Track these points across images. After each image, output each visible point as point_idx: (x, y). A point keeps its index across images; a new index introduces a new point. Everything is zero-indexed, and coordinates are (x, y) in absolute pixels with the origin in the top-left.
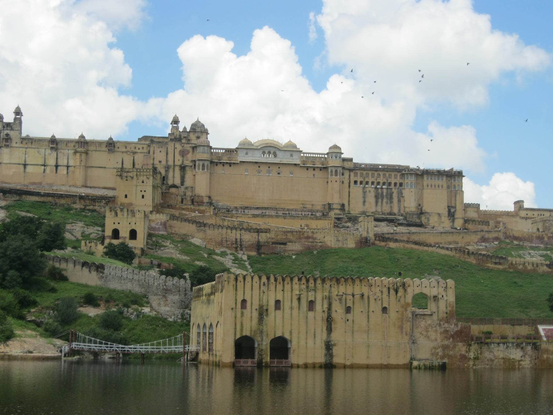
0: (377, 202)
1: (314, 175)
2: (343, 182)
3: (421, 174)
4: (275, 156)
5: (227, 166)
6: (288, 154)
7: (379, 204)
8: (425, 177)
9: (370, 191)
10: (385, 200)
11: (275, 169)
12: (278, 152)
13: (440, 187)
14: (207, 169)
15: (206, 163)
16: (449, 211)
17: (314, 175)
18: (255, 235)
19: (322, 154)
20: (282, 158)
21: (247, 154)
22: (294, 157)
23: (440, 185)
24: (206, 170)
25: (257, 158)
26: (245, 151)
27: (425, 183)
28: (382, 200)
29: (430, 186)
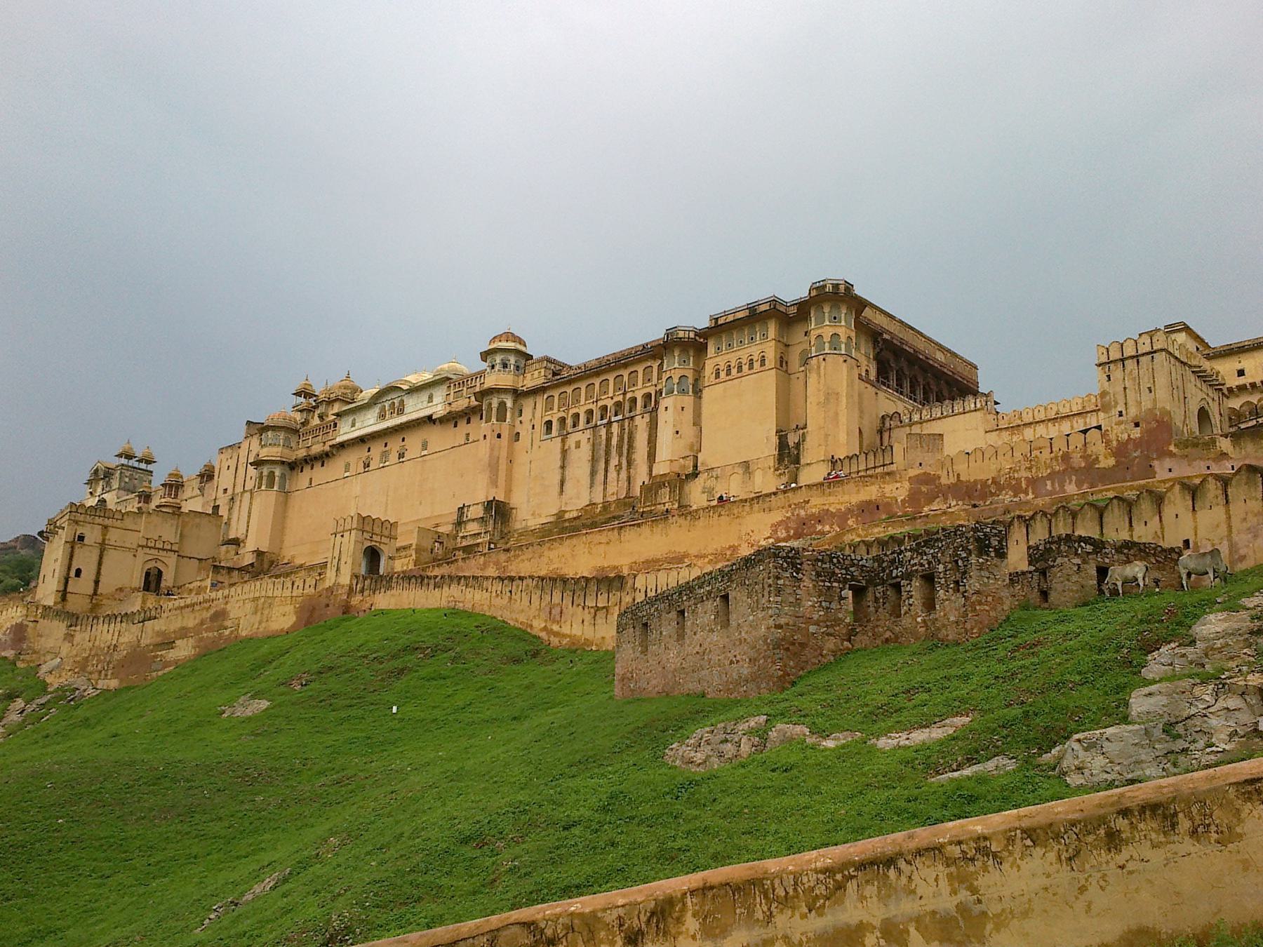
0: (593, 473)
4: (401, 411)
5: (318, 465)
7: (600, 477)
8: (711, 350)
9: (578, 445)
10: (614, 461)
11: (395, 445)
13: (757, 365)
14: (271, 484)
15: (266, 471)
16: (783, 445)
17: (468, 435)
18: (135, 629)
20: (416, 408)
21: (353, 425)
22: (436, 400)
24: (263, 487)
28: (607, 462)
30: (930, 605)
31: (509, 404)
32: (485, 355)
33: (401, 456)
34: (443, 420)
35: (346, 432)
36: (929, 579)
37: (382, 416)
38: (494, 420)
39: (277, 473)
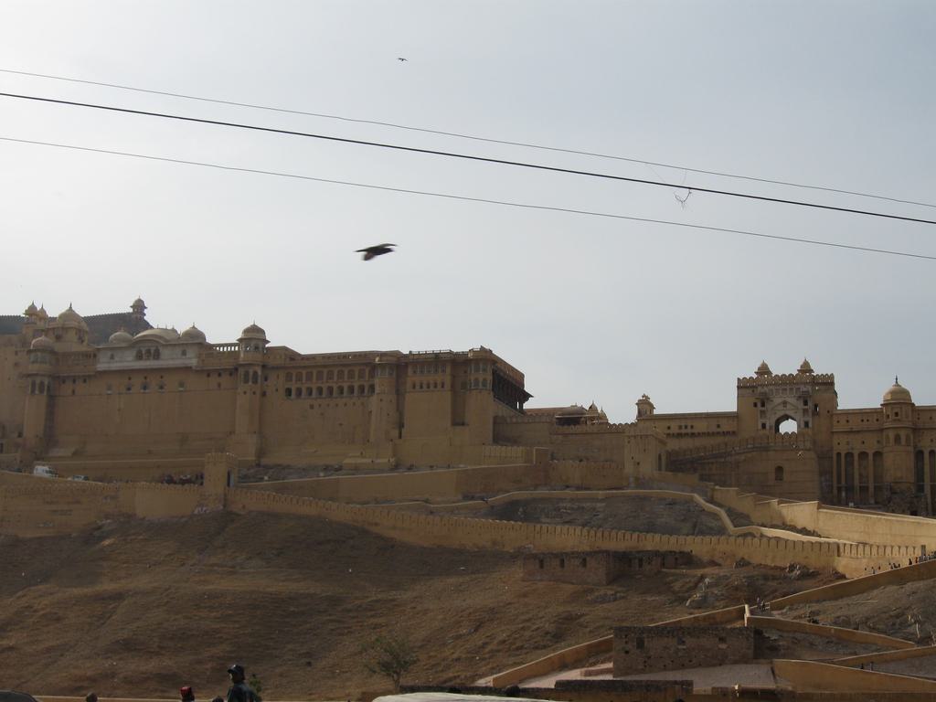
1: (219, 385)
2: (264, 394)
3: (399, 366)
4: (157, 356)
6: (178, 351)
8: (410, 371)
9: (312, 407)
12: (161, 349)
13: (439, 386)
17: (219, 385)
19: (231, 345)
20: (169, 359)
21: (112, 357)
23: (439, 382)
24: (37, 392)
25: (126, 364)
26: (109, 353)
27: (409, 381)
29: (418, 387)
30: (640, 566)
31: (260, 373)
32: (240, 340)
33: (161, 388)
34: (199, 372)
35: (103, 364)
36: (641, 560)
37: (139, 357)
38: (250, 383)
39: (46, 383)
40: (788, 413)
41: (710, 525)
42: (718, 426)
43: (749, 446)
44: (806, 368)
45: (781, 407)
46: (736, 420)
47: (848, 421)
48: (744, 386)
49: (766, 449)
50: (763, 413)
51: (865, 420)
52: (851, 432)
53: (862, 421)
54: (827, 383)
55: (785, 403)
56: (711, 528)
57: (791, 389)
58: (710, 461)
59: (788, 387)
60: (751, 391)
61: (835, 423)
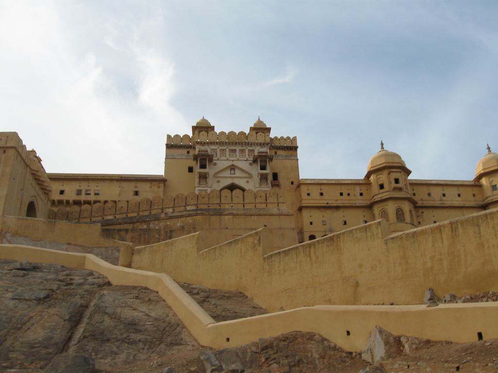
40: (241, 183)
41: (128, 314)
42: (136, 193)
43: (189, 208)
44: (261, 129)
45: (227, 173)
46: (162, 185)
47: (322, 194)
48: (173, 145)
49: (219, 213)
50: (203, 177)
51: (345, 194)
52: (328, 207)
53: (341, 194)
54: (290, 148)
55: (233, 168)
56: (133, 326)
57: (242, 151)
58: (125, 226)
59: (238, 148)
60: (185, 151)
61: (304, 196)
